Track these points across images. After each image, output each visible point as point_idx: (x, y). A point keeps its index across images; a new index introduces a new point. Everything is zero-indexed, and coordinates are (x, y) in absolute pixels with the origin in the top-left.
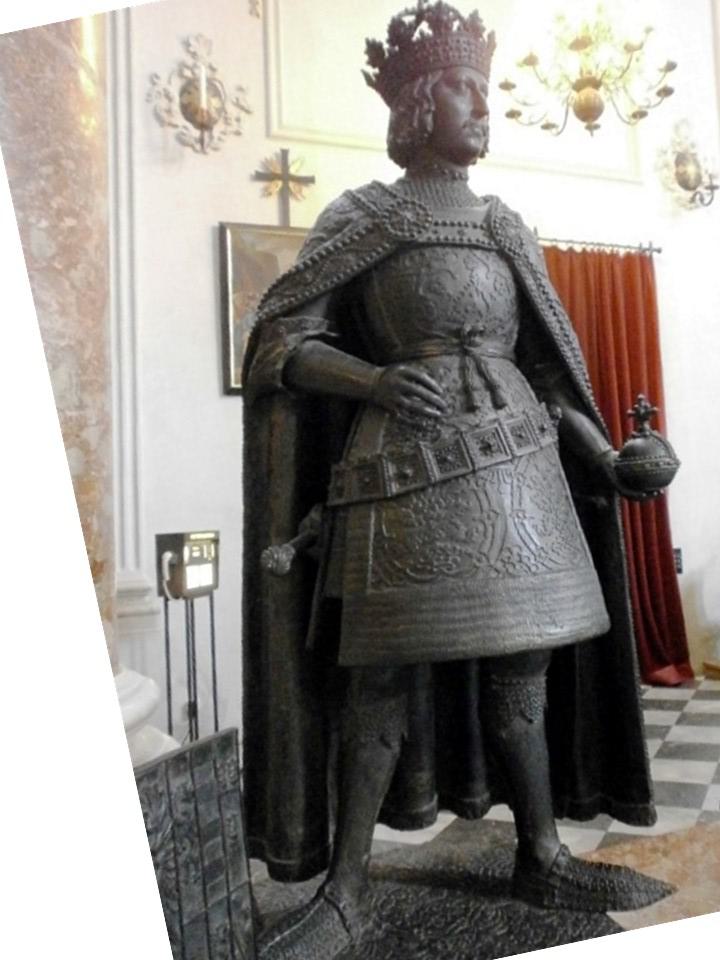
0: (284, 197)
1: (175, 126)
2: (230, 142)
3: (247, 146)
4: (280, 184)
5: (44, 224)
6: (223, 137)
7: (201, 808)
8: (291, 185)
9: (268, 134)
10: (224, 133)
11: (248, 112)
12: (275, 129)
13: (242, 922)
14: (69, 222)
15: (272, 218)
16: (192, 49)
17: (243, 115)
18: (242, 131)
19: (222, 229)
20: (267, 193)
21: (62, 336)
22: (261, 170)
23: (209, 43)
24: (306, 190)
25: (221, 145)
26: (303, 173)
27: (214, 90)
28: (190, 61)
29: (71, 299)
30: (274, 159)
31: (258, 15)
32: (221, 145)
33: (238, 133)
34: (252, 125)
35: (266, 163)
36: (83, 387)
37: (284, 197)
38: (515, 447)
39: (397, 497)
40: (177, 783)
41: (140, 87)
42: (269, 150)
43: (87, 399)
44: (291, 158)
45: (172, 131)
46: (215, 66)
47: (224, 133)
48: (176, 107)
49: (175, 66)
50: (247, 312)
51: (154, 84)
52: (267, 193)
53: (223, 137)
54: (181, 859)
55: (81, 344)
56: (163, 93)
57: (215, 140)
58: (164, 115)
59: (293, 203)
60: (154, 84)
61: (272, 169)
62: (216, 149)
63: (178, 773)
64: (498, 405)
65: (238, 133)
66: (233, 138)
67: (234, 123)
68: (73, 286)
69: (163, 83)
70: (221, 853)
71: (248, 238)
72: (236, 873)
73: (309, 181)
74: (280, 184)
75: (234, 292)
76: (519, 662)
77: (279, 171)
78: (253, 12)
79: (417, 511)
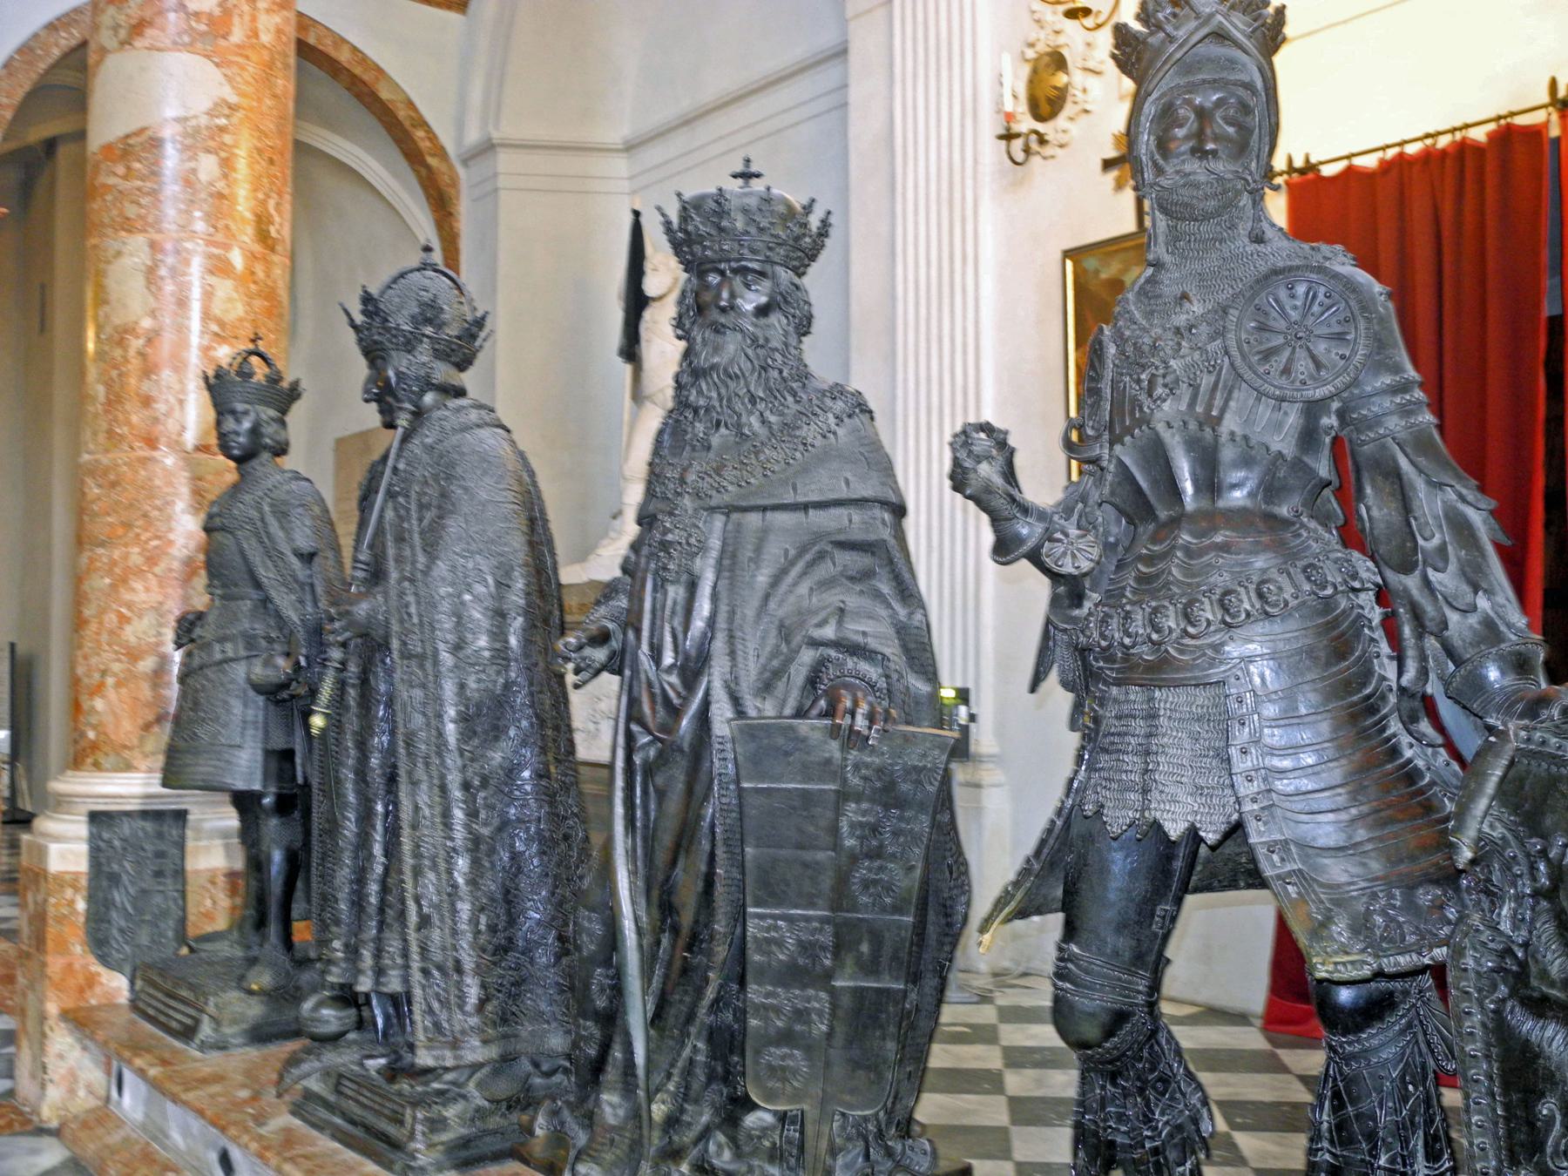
16: (1036, 16)
18: (1088, 107)
65: (1086, 111)
66: (1084, 115)
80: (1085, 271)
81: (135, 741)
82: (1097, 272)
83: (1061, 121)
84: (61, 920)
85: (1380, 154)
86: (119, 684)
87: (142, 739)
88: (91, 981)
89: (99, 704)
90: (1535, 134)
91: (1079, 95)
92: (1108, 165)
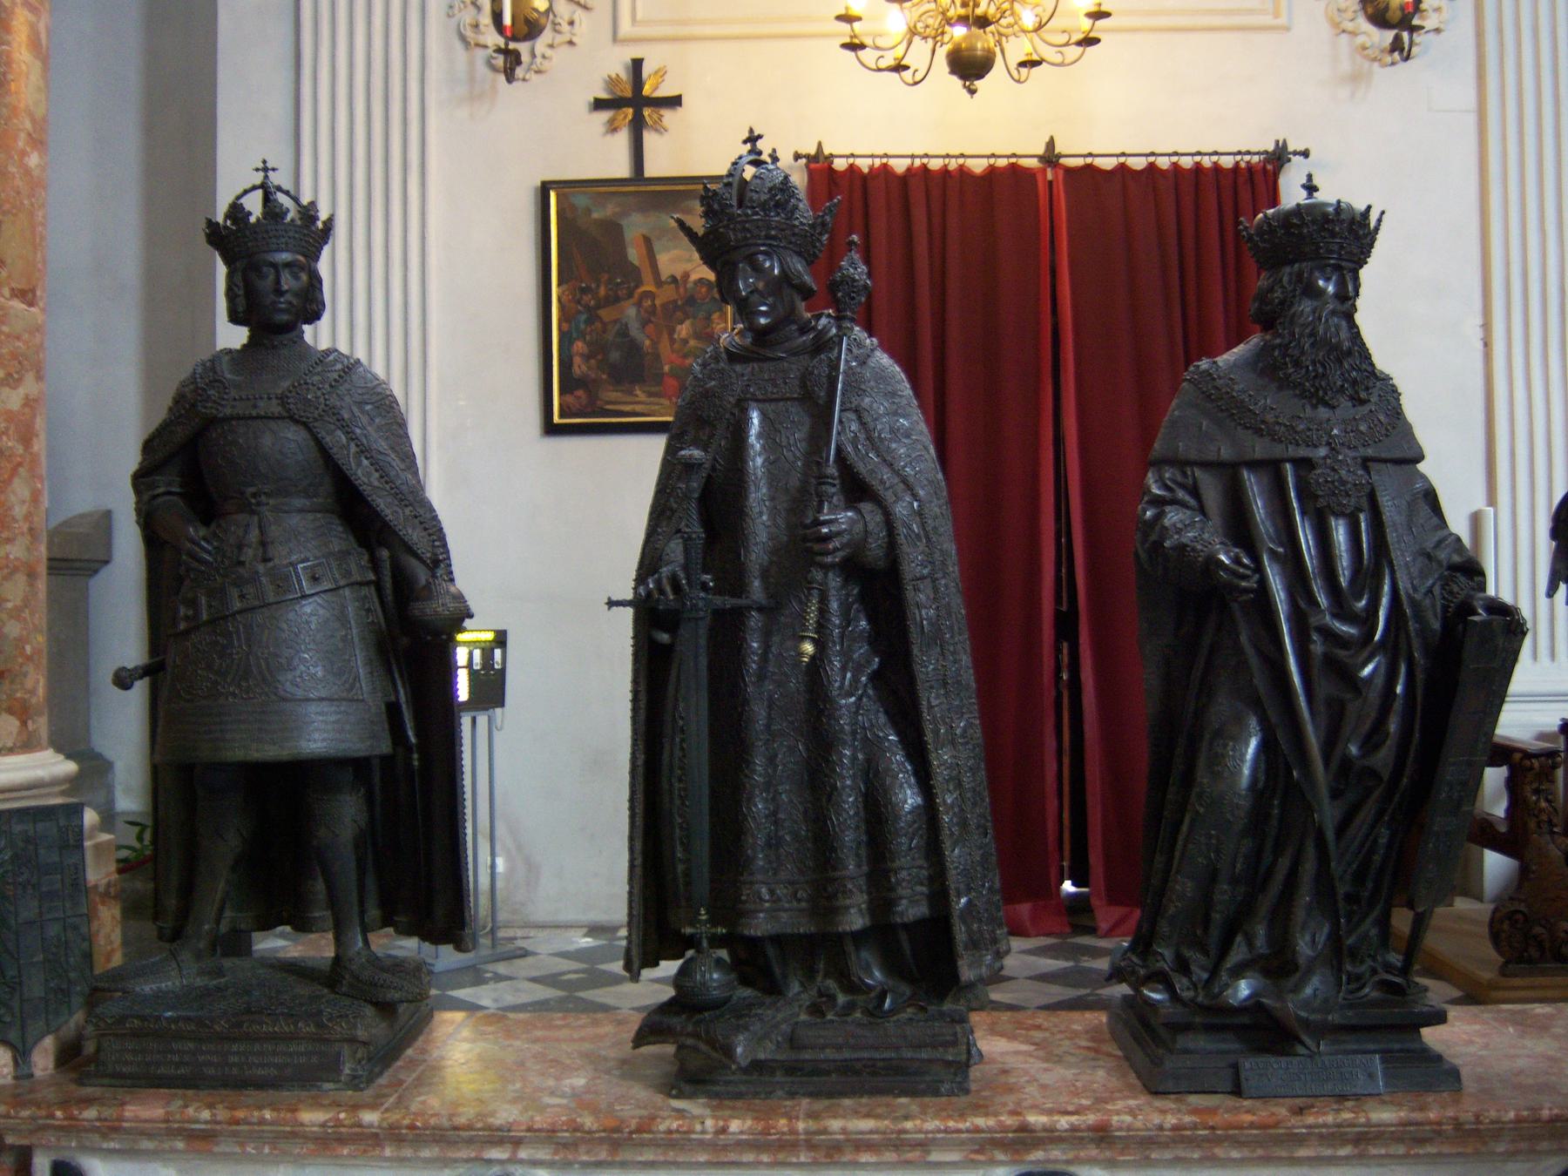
0: (637, 129)
2: (560, 56)
3: (580, 63)
6: (549, 52)
8: (646, 112)
9: (615, 38)
11: (585, 7)
12: (625, 27)
15: (620, 167)
17: (579, 14)
18: (575, 39)
19: (545, 188)
20: (612, 128)
22: (604, 95)
24: (668, 116)
26: (665, 91)
30: (624, 76)
32: (546, 65)
33: (571, 43)
35: (612, 82)
37: (637, 129)
39: (187, 632)
42: (616, 63)
44: (647, 70)
45: (481, 55)
47: (551, 46)
48: (486, 19)
50: (580, 312)
52: (612, 128)
53: (549, 52)
57: (539, 60)
58: (469, 33)
59: (649, 138)
62: (538, 72)
65: (571, 43)
66: (566, 49)
71: (581, 201)
73: (675, 102)
74: (630, 111)
75: (559, 285)
77: (628, 94)
80: (573, 208)
82: (589, 211)
83: (541, 44)
85: (909, 161)
90: (1028, 173)
91: (565, 27)
92: (599, 105)
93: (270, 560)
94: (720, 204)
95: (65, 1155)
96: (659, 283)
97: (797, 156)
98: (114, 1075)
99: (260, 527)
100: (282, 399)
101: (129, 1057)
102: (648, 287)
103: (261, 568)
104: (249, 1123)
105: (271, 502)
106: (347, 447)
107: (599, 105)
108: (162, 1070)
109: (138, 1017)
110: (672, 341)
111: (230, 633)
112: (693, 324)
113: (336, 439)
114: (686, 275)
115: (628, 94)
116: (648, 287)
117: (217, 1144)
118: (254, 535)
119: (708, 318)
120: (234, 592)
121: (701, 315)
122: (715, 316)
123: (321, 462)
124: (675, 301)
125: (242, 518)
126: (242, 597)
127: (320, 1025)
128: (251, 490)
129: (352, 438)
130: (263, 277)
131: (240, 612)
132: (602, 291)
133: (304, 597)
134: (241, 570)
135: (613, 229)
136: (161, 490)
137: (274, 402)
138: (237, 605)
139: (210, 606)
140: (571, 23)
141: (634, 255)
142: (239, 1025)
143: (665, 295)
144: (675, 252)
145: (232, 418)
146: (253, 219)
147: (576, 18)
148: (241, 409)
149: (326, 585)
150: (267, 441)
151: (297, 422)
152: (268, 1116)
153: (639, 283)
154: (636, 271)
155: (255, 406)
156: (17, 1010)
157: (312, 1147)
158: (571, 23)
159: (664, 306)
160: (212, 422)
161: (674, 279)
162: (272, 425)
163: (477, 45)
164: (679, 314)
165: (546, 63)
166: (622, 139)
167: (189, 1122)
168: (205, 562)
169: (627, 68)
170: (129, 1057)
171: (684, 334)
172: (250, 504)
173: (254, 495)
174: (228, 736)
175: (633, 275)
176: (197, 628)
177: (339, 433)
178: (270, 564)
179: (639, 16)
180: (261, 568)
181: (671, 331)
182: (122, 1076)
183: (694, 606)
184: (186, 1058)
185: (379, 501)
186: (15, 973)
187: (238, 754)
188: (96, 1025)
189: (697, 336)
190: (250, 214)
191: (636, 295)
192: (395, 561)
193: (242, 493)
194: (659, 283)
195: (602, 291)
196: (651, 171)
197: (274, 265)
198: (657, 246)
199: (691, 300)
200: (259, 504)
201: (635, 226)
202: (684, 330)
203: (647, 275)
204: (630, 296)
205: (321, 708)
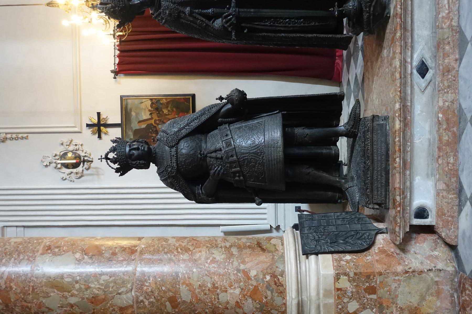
1: (83, 170)
4: (102, 128)
5: (181, 256)
7: (314, 225)
8: (102, 123)
9: (80, 132)
10: (83, 151)
11: (71, 141)
13: (342, 215)
14: (179, 250)
16: (48, 164)
17: (74, 143)
21: (206, 252)
22: (97, 135)
23: (44, 157)
24: (103, 116)
25: (88, 152)
27: (64, 156)
28: (54, 165)
29: (197, 249)
30: (91, 130)
31: (27, 136)
34: (77, 139)
35: (94, 133)
36: (217, 247)
38: (231, 148)
40: (306, 232)
41: (67, 184)
42: (88, 132)
43: (219, 246)
44: (90, 123)
45: (85, 172)
46: (54, 155)
47: (83, 151)
48: (74, 170)
49: (56, 170)
51: (66, 179)
54: (323, 231)
55: (207, 247)
56: (69, 176)
57: (86, 154)
58: (79, 175)
59: (109, 122)
60: (66, 179)
61: (95, 131)
62: (90, 155)
63: (304, 231)
64: (220, 150)
65: (82, 145)
67: (77, 147)
68: (194, 249)
69: (65, 176)
70: (325, 221)
72: (331, 217)
73: (99, 114)
74: (102, 128)
76: (288, 139)
77: (97, 128)
78: (26, 138)
79: (247, 173)
81: (270, 254)
83: (82, 154)
84: (357, 267)
86: (244, 262)
87: (269, 252)
88: (382, 251)
89: (253, 273)
92: (100, 137)
93: (221, 149)
94: (111, 8)
95: (413, 213)
96: (152, 118)
97: (115, 78)
98: (386, 197)
99: (211, 153)
100: (171, 147)
101: (379, 192)
102: (153, 121)
103: (223, 152)
104: (400, 145)
105: (203, 150)
106: (186, 129)
107: (100, 137)
108: (383, 181)
109: (367, 190)
110: (169, 115)
111: (244, 159)
112: (164, 108)
113: (184, 132)
114: (149, 110)
115: (97, 128)
116: (153, 121)
117: (407, 160)
118: (214, 155)
119: (162, 104)
120: (231, 159)
121: (161, 106)
122: (161, 102)
123: (191, 137)
124: (157, 114)
125: (208, 159)
126: (232, 156)
127: (368, 131)
128: (199, 156)
129: (184, 128)
130: (133, 154)
131: (237, 157)
132: (154, 135)
133: (232, 138)
134: (224, 158)
135: (136, 132)
136: (200, 191)
137: (172, 150)
138: (235, 157)
139: (235, 167)
140: (76, 145)
141: (144, 126)
142: (368, 157)
143: (155, 117)
144: (143, 114)
145: (177, 163)
146: (115, 156)
147: (74, 144)
148: (174, 160)
149: (229, 132)
150: (184, 151)
151: (178, 144)
152: (398, 139)
153: (152, 124)
154: (148, 125)
155: (173, 156)
156: (365, 231)
157: (407, 129)
158: (76, 145)
159: (158, 117)
160: (178, 170)
161: (150, 114)
162: (179, 150)
163: (82, 173)
164: (161, 113)
165: (87, 152)
166: (110, 130)
167: (400, 166)
168: (221, 169)
169: (89, 129)
170: (379, 192)
171: (167, 111)
172: (204, 157)
173: (201, 155)
174: (276, 158)
175: (149, 126)
176: (242, 172)
177: (182, 131)
178: (222, 149)
179: (74, 125)
180: (223, 152)
181: (166, 115)
182: (386, 194)
183: (235, 11)
184: (379, 174)
185: (203, 119)
186: (353, 232)
187: (281, 154)
188: (369, 204)
189: (167, 107)
190: (114, 157)
191: (155, 125)
192: (222, 117)
193: (201, 158)
194: (152, 118)
195: (154, 135)
196: (119, 122)
197: (130, 150)
198: (141, 119)
199: (157, 109)
200: (204, 154)
201: (135, 126)
202: (165, 111)
203: (149, 122)
204: (155, 127)
205: (268, 135)
